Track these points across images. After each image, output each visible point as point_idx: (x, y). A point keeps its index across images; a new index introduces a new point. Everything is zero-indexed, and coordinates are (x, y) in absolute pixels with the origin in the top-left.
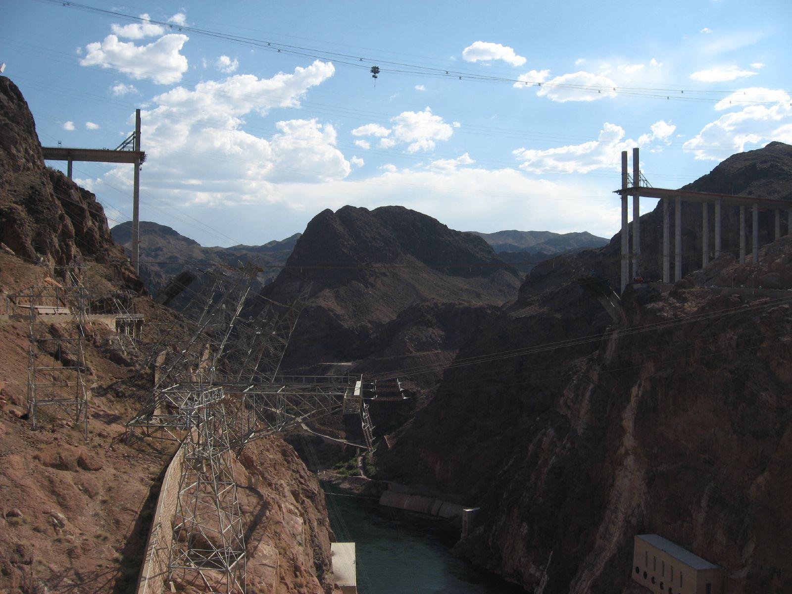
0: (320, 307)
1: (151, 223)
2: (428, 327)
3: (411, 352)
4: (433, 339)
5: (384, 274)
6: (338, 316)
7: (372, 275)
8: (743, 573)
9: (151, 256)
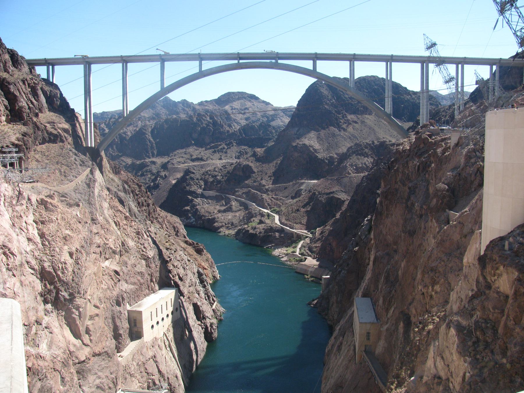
1: (243, 92)
2: (365, 157)
3: (350, 174)
4: (366, 165)
5: (356, 122)
6: (315, 150)
7: (345, 123)
8: (385, 327)
9: (242, 113)
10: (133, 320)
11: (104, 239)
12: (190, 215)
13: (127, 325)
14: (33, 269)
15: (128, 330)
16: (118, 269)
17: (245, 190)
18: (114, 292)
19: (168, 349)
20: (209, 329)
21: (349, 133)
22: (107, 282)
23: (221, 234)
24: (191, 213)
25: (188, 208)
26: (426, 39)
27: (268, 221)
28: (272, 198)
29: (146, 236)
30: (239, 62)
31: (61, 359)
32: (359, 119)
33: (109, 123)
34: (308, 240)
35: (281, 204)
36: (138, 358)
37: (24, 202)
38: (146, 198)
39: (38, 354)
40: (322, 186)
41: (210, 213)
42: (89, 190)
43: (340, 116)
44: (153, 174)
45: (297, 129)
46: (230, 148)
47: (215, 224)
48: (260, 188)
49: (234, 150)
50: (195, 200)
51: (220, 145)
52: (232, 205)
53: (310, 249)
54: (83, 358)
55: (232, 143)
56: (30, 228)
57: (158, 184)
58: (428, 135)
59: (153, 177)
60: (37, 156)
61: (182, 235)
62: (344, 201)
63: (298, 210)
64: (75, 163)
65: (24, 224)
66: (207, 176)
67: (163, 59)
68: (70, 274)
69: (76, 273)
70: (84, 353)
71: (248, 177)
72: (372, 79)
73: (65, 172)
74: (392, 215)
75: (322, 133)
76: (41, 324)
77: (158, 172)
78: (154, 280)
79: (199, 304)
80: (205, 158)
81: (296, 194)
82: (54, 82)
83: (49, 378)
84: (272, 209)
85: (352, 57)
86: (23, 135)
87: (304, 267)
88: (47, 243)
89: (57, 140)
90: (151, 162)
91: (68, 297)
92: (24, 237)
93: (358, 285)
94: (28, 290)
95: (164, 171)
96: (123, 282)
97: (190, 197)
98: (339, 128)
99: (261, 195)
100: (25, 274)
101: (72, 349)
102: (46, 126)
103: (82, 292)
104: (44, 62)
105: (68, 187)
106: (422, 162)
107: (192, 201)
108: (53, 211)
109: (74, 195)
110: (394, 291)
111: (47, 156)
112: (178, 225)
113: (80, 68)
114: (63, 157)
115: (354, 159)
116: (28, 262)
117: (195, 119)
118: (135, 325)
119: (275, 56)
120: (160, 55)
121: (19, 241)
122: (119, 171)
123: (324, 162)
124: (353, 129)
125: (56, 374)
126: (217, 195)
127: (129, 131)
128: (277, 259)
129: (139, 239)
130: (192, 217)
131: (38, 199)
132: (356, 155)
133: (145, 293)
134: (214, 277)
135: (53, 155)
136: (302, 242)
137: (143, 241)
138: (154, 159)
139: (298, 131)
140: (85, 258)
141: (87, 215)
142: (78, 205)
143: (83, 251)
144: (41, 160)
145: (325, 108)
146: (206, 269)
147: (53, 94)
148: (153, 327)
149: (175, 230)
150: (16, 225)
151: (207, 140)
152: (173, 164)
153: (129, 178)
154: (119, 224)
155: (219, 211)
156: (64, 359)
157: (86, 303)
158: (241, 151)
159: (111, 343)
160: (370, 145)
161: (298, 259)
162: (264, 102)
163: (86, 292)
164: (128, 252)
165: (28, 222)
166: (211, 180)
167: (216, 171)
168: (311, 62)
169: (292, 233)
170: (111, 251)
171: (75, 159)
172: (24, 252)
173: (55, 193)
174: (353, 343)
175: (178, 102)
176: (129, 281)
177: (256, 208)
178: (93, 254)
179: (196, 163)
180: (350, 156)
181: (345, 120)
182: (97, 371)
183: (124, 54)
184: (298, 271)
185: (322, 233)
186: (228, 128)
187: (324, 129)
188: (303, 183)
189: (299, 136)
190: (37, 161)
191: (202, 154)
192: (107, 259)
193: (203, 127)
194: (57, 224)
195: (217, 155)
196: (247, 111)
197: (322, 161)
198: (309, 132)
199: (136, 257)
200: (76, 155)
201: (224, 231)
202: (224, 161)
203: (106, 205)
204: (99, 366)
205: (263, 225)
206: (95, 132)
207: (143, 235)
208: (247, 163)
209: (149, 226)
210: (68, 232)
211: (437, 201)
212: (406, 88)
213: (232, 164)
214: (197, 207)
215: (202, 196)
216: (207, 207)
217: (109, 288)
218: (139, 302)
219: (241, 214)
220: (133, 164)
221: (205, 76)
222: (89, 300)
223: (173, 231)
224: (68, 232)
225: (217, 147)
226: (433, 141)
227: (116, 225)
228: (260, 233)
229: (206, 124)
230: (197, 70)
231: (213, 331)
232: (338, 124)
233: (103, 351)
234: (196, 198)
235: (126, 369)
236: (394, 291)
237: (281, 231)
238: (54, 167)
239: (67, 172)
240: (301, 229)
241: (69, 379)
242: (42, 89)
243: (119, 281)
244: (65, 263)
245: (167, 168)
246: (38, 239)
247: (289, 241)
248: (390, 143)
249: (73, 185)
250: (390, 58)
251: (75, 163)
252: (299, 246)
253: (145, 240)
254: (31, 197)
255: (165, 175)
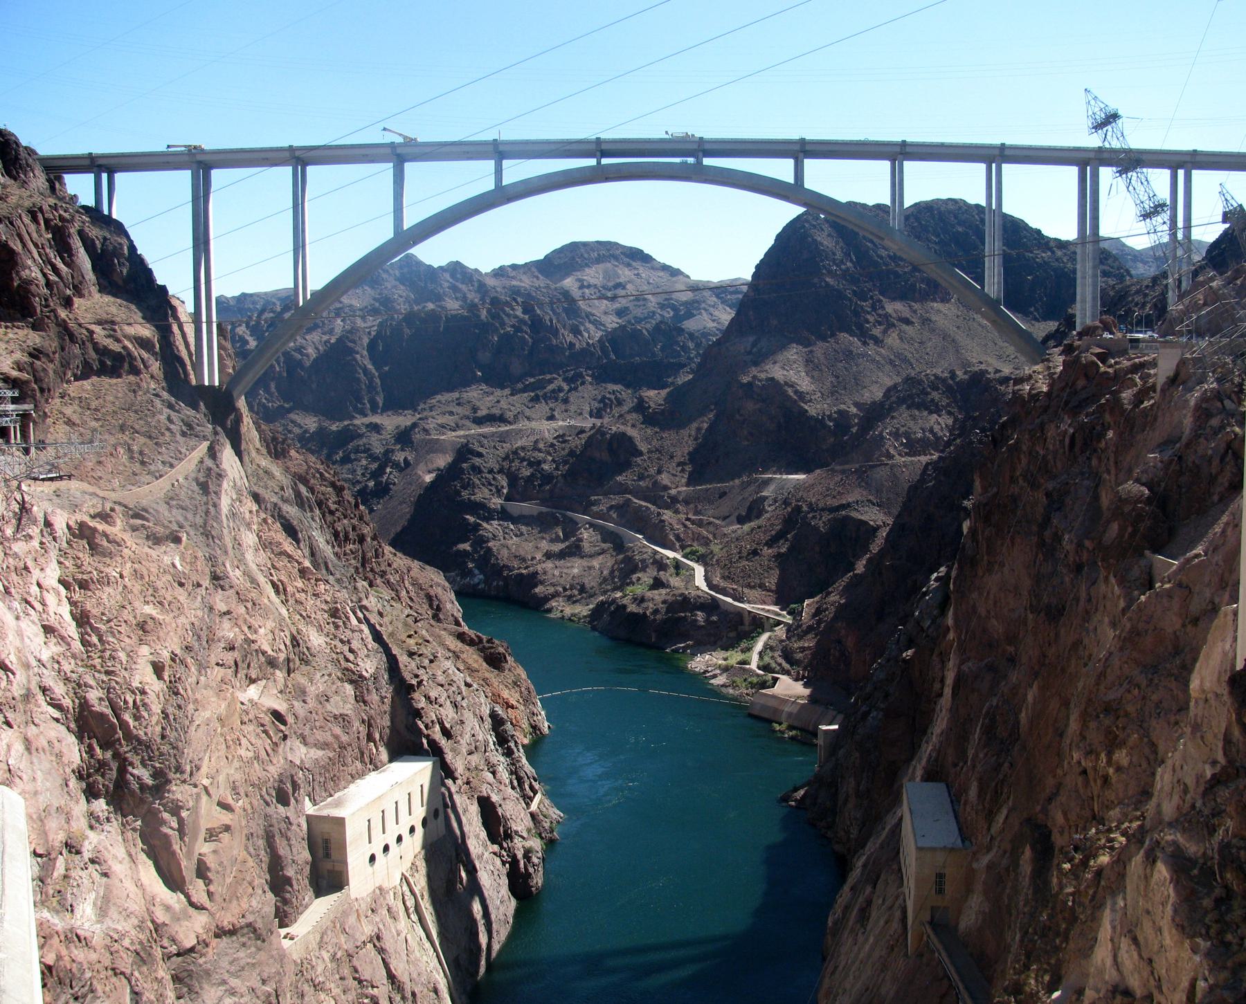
0: (773, 379)
1: (609, 243)
2: (931, 412)
3: (891, 457)
4: (934, 434)
5: (907, 322)
6: (801, 395)
7: (880, 323)
9: (607, 298)
10: (320, 841)
11: (246, 629)
12: (471, 565)
13: (306, 855)
14: (59, 707)
15: (308, 868)
16: (281, 707)
17: (616, 500)
18: (271, 768)
19: (414, 917)
20: (522, 865)
21: (891, 348)
22: (252, 741)
23: (552, 615)
24: (473, 561)
25: (466, 546)
26: (1093, 102)
27: (675, 582)
28: (688, 519)
29: (354, 621)
30: (599, 163)
31: (132, 943)
32: (915, 312)
33: (258, 323)
34: (780, 632)
35: (711, 537)
36: (335, 940)
37: (34, 531)
38: (355, 521)
39: (71, 930)
40: (819, 488)
41: (524, 560)
42: (205, 498)
43: (866, 305)
44: (373, 458)
45: (751, 339)
46: (576, 389)
47: (537, 590)
48: (655, 494)
49: (587, 395)
50: (485, 525)
51: (550, 381)
52: (581, 540)
53: (787, 655)
54: (189, 942)
55: (581, 376)
56: (51, 599)
57: (388, 484)
58: (1097, 355)
59: (374, 466)
60: (68, 411)
61: (451, 619)
62: (876, 529)
63: (755, 553)
64: (168, 429)
65: (35, 589)
66: (517, 463)
67: (400, 155)
68: (154, 719)
69: (172, 717)
70: (191, 929)
71: (625, 466)
72: (951, 207)
73: (141, 453)
74: (1002, 565)
75: (820, 349)
76: (78, 852)
77: (387, 452)
78: (377, 736)
79: (495, 798)
80: (509, 415)
81: (750, 509)
82: (115, 216)
83: (100, 993)
84: (688, 550)
85: (898, 149)
86: (30, 355)
87: (772, 703)
88: (95, 639)
89: (122, 367)
90: (367, 426)
91: (150, 782)
92: (33, 622)
93: (914, 749)
94: (44, 763)
95: (403, 450)
96: (294, 742)
97: (471, 519)
98: (864, 335)
99: (659, 514)
100: (36, 721)
101: (161, 916)
102: (91, 332)
103: (188, 768)
104: (87, 162)
105: (150, 492)
106: (1082, 426)
107: (477, 527)
108: (110, 555)
109: (166, 513)
110: (1006, 765)
111: (96, 410)
112: (439, 591)
113: (182, 180)
114: (136, 412)
115: (904, 419)
116: (44, 690)
117: (484, 314)
118: (328, 855)
119: (695, 146)
120: (392, 145)
121: (20, 634)
122: (283, 450)
123: (825, 426)
124: (901, 339)
125: (118, 984)
126: (542, 513)
127: (312, 345)
128: (699, 680)
129: (337, 627)
130: (476, 572)
131: (72, 523)
132: (908, 408)
133: (352, 769)
134: (535, 727)
135: (110, 408)
136: (765, 637)
137: (348, 632)
138: (376, 419)
139: (754, 344)
140: (194, 679)
141: (201, 564)
142: (177, 540)
143: (189, 660)
144: (78, 422)
145: (827, 284)
146: (512, 707)
147: (111, 248)
148: (372, 858)
149: (431, 606)
150: (13, 590)
151: (516, 367)
152: (426, 431)
153: (309, 467)
154: (285, 590)
155: (549, 556)
156: (141, 943)
157: (198, 795)
158: (604, 397)
159: (265, 902)
160: (944, 380)
161: (755, 680)
162: (665, 268)
163: (198, 768)
164: (307, 663)
165: (45, 583)
166: (526, 472)
167: (540, 451)
168: (789, 164)
169: (740, 614)
170: (263, 659)
171: (169, 419)
172: (34, 663)
173: (117, 508)
174: (900, 901)
175: (441, 268)
176: (310, 740)
177: (645, 546)
178: (217, 668)
179: (487, 429)
180: (891, 409)
181: (880, 315)
182: (226, 976)
183: (297, 143)
184: (755, 712)
185: (818, 612)
186: (570, 338)
187: (824, 339)
188: (767, 482)
189: (758, 359)
190: (70, 423)
191: (503, 404)
192: (252, 681)
193: (507, 334)
194: (121, 589)
195: (543, 408)
196: (621, 292)
197: (818, 423)
198: (783, 347)
199: (330, 675)
200: (171, 407)
201: (562, 608)
202: (561, 423)
203: (249, 539)
204: (231, 963)
205: (663, 591)
206: (220, 347)
207: (348, 618)
208: (622, 428)
209: (362, 595)
210: (149, 610)
211: (1122, 529)
212: (1038, 232)
213: (582, 431)
214: (490, 544)
215: (504, 515)
216: (515, 545)
217: (257, 758)
218: (337, 795)
219: (603, 563)
220: (321, 431)
221: (510, 199)
222: (206, 788)
223: (426, 606)
224: (149, 610)
225: (541, 385)
226: (1111, 370)
227: (277, 592)
228: (656, 612)
229: (513, 326)
230: (489, 185)
231: (531, 870)
232: (860, 327)
233: (243, 922)
234: (488, 519)
235: (302, 969)
236: (1006, 765)
237: (711, 606)
238: (112, 440)
239: (146, 451)
240: (764, 603)
241: (152, 997)
242: (81, 233)
243: (285, 738)
244: (143, 692)
245: (412, 443)
246: (71, 629)
247: (732, 634)
248: (998, 375)
249: (163, 485)
250: (997, 152)
251: (168, 429)
252: (759, 646)
253: (353, 631)
254: (52, 519)
255: (405, 459)
